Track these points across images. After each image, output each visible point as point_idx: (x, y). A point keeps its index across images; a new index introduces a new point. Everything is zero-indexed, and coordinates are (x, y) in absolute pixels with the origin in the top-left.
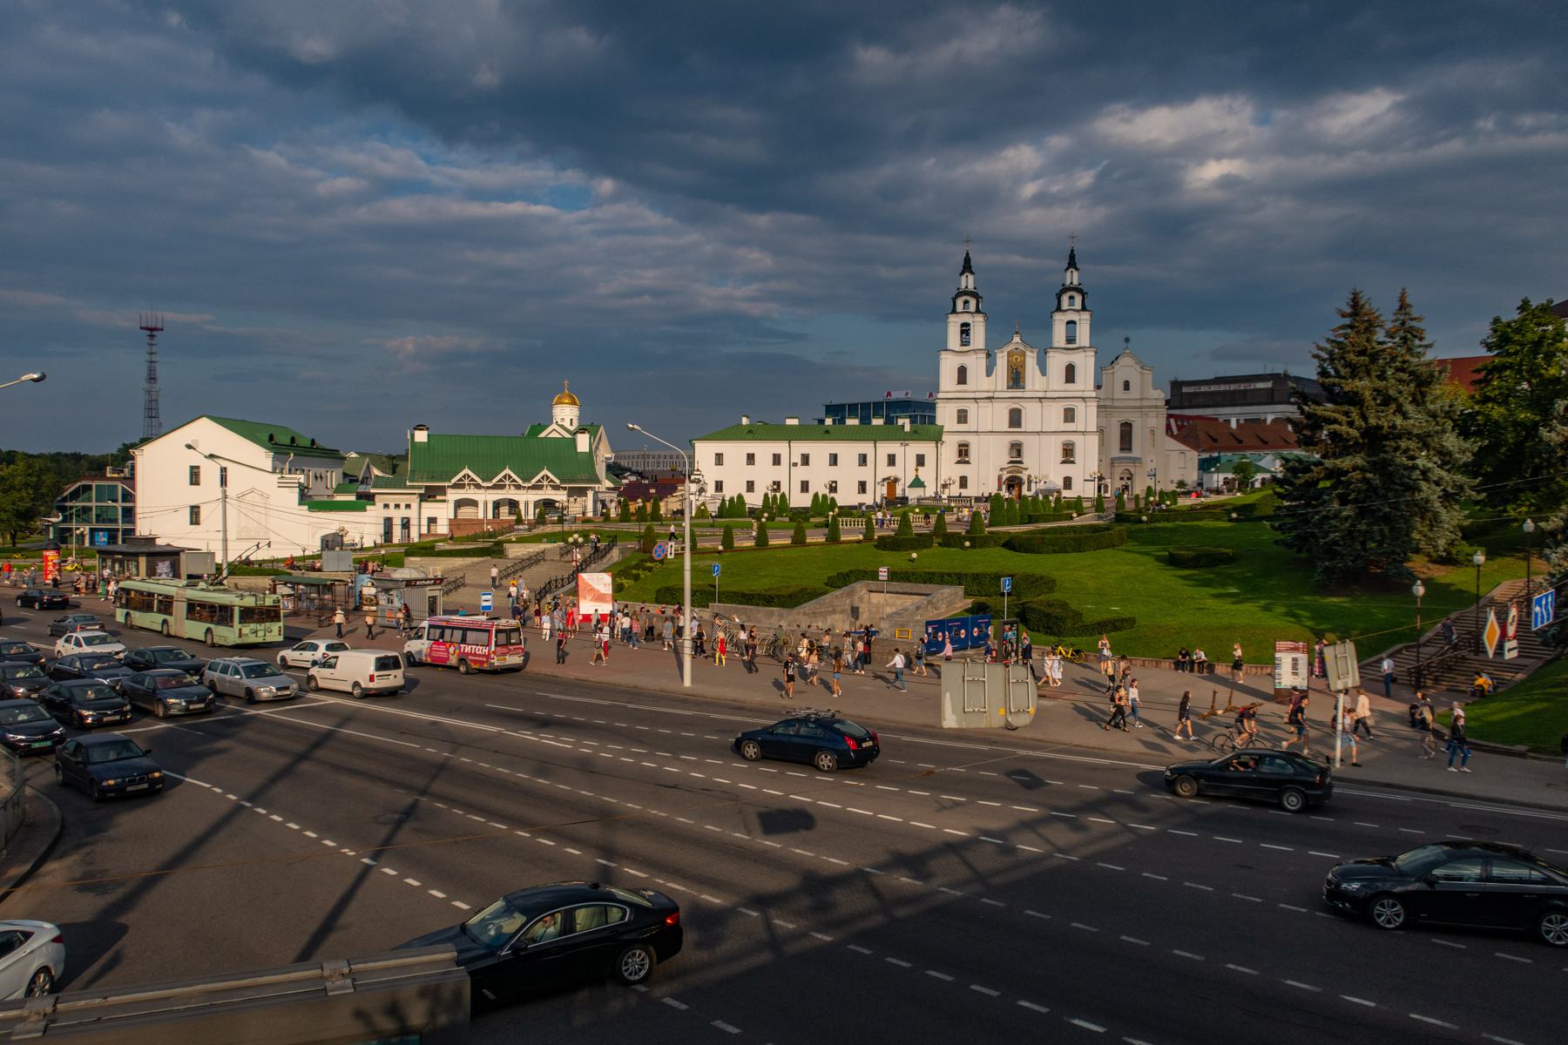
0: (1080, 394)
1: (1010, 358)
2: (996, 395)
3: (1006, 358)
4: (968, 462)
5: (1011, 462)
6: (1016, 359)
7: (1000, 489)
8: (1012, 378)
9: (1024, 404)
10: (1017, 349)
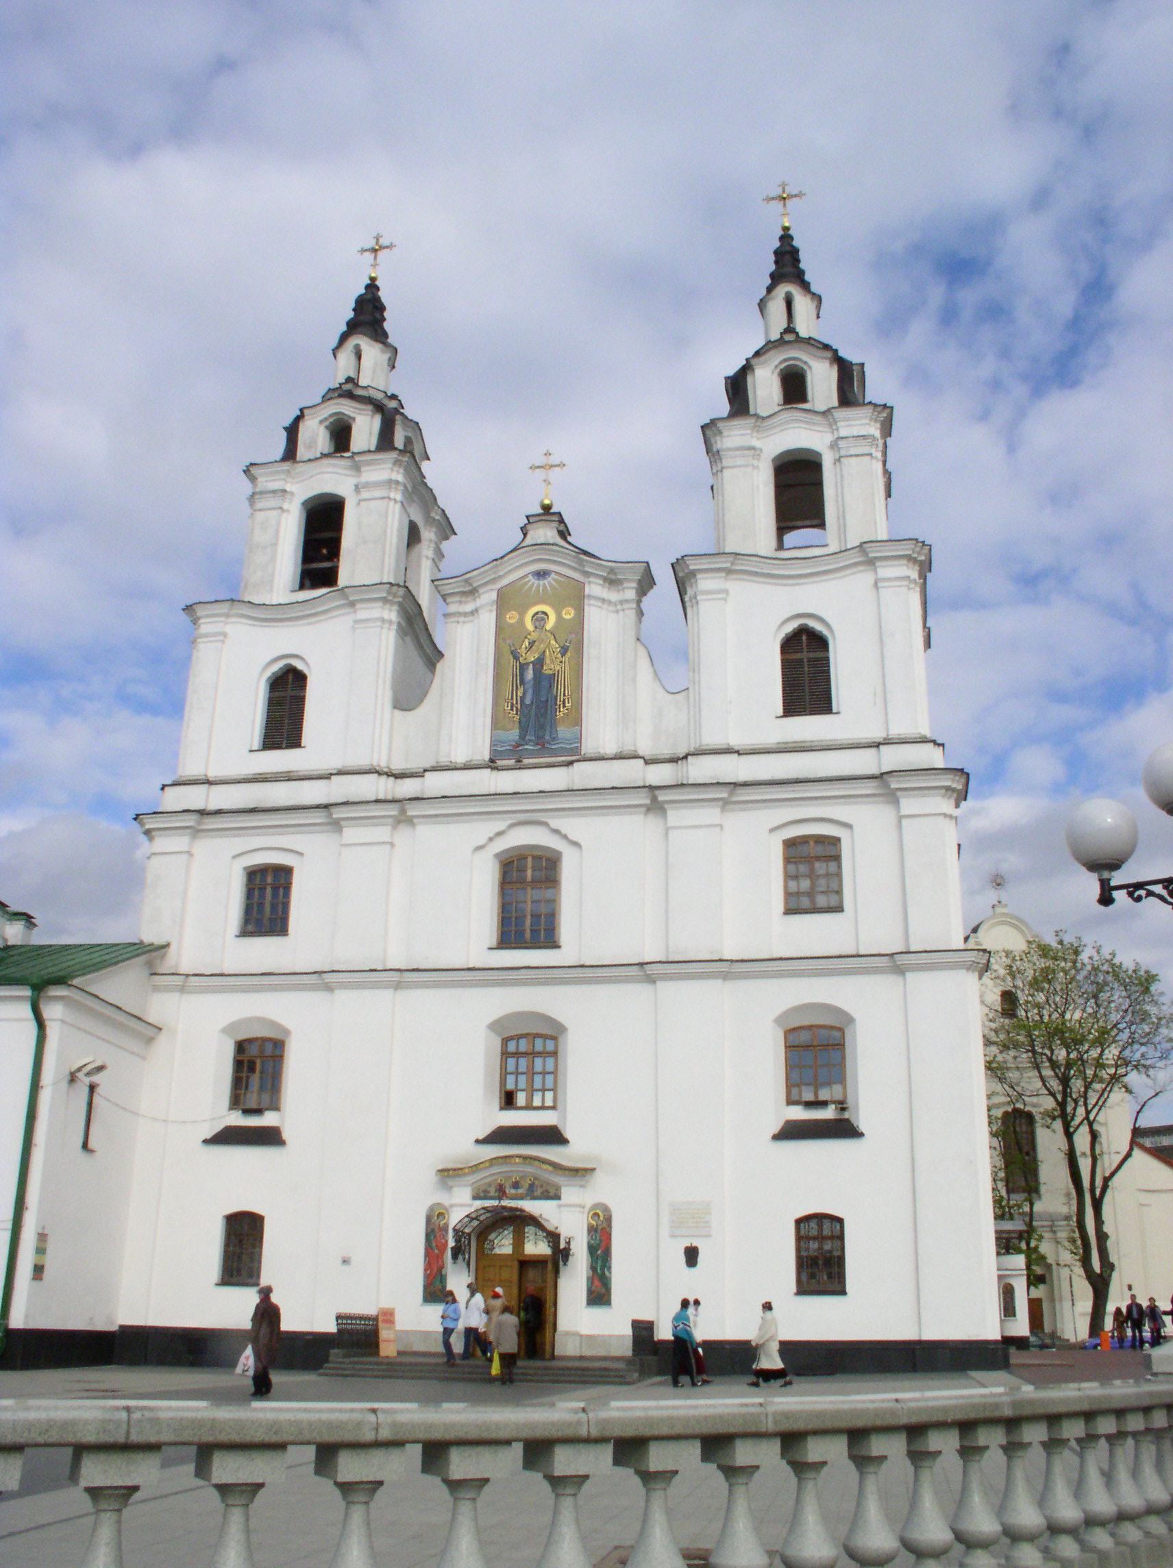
0: (863, 762)
1: (511, 618)
2: (435, 783)
3: (488, 620)
4: (270, 1137)
5: (502, 1136)
6: (540, 618)
7: (436, 1291)
8: (524, 710)
9: (573, 826)
10: (541, 574)
